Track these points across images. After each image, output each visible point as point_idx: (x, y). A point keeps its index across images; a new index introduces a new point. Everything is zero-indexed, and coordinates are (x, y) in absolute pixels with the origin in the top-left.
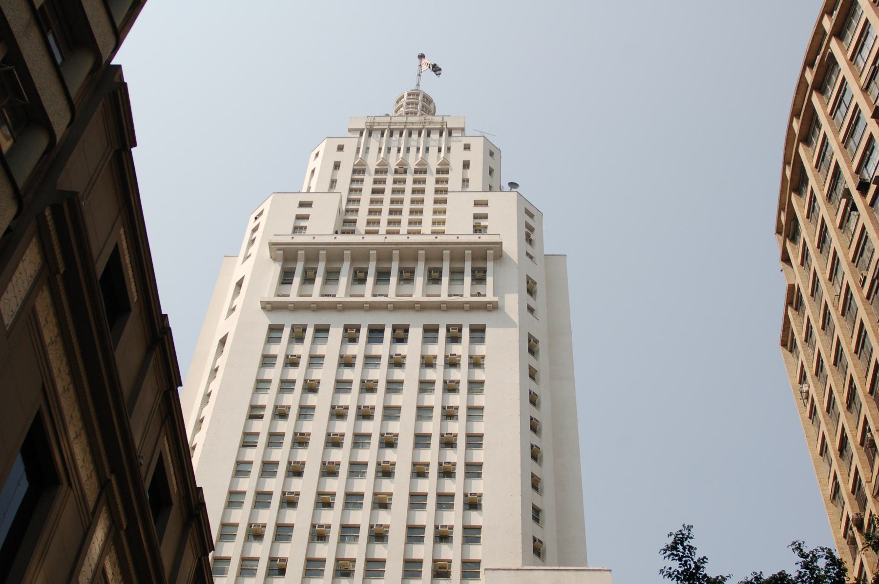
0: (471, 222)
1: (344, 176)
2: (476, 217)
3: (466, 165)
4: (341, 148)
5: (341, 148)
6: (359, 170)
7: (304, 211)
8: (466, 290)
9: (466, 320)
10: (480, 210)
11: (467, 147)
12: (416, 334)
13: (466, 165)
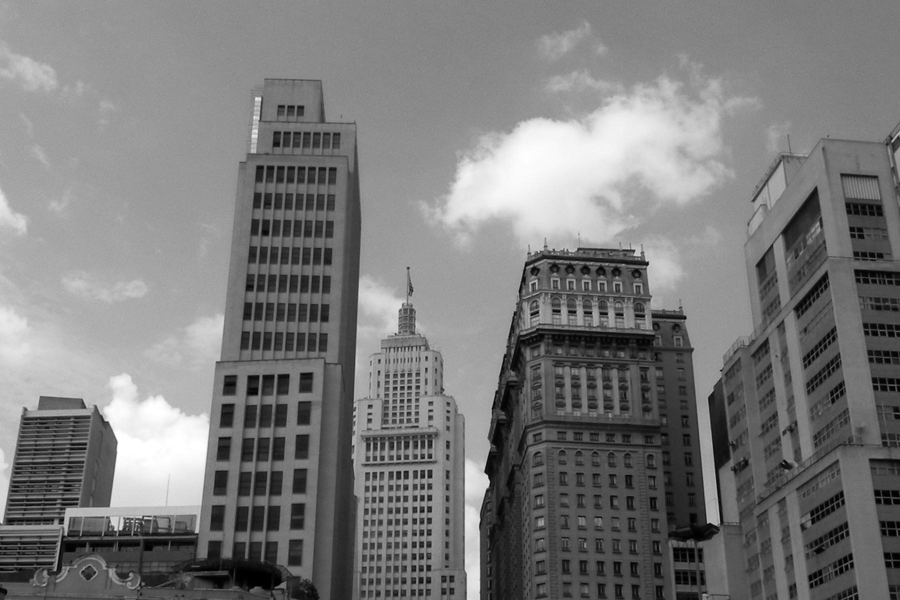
0: (427, 414)
1: (382, 378)
2: (430, 411)
3: (426, 369)
4: (379, 361)
5: (379, 361)
6: (387, 376)
7: (370, 411)
8: (426, 451)
9: (426, 468)
10: (431, 408)
11: (427, 358)
12: (411, 475)
13: (426, 369)
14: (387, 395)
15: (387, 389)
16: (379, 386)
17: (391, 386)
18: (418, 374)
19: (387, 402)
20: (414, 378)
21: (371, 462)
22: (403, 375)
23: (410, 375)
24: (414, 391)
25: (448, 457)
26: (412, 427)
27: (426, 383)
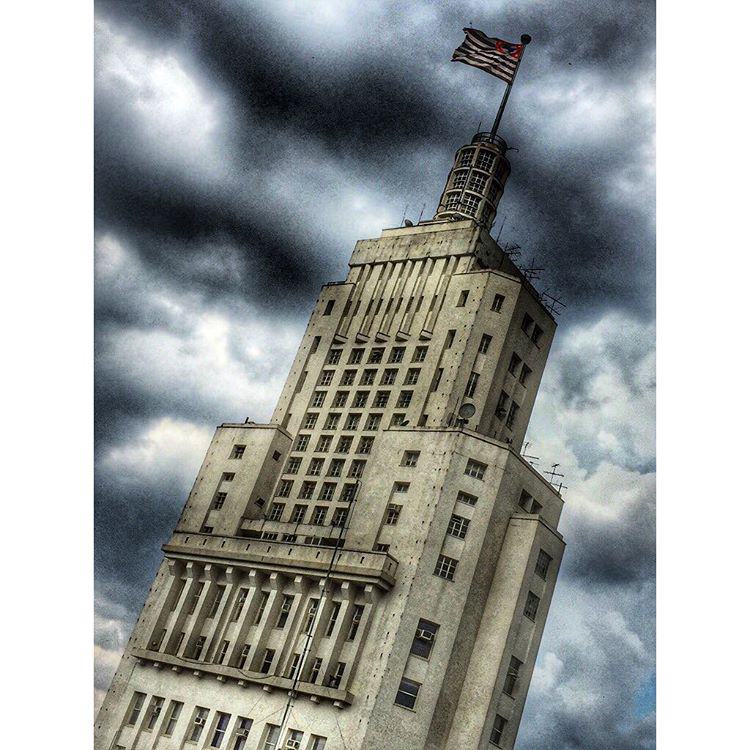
3: (452, 333)
10: (404, 475)
13: (452, 333)
14: (311, 418)
15: (318, 398)
16: (298, 389)
17: (332, 389)
18: (421, 352)
19: (302, 442)
20: (405, 365)
21: (160, 656)
22: (376, 356)
23: (398, 354)
24: (390, 410)
25: (407, 696)
26: (328, 542)
27: (434, 387)
